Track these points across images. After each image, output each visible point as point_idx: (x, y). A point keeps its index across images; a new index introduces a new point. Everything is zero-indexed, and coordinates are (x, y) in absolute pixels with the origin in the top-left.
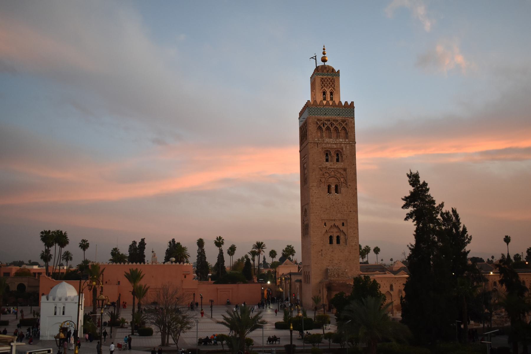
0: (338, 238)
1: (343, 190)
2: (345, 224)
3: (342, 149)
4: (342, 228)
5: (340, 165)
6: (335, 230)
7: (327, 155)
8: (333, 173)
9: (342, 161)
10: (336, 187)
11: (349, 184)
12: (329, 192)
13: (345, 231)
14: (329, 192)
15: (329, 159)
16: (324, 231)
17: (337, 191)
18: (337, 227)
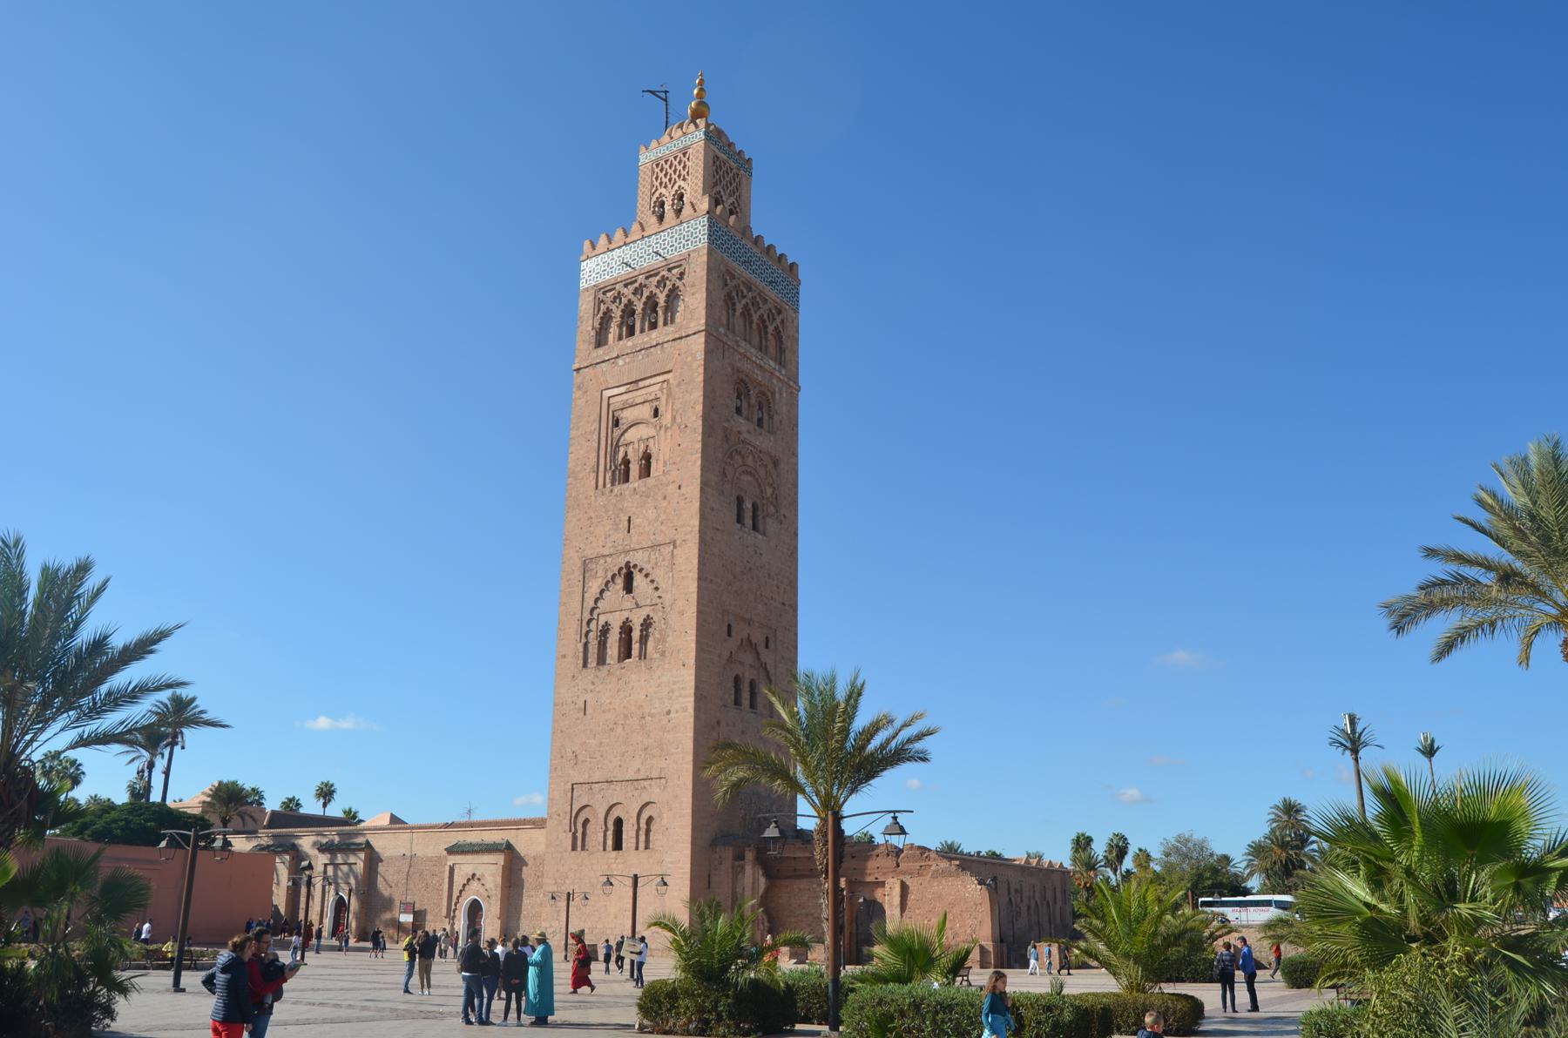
0: (752, 684)
1: (771, 525)
2: (771, 644)
3: (773, 394)
4: (766, 656)
5: (763, 441)
6: (748, 658)
7: (738, 397)
8: (750, 461)
9: (772, 432)
10: (755, 507)
11: (783, 511)
12: (740, 520)
13: (770, 667)
14: (740, 520)
15: (744, 412)
16: (726, 654)
17: (755, 528)
18: (753, 647)
